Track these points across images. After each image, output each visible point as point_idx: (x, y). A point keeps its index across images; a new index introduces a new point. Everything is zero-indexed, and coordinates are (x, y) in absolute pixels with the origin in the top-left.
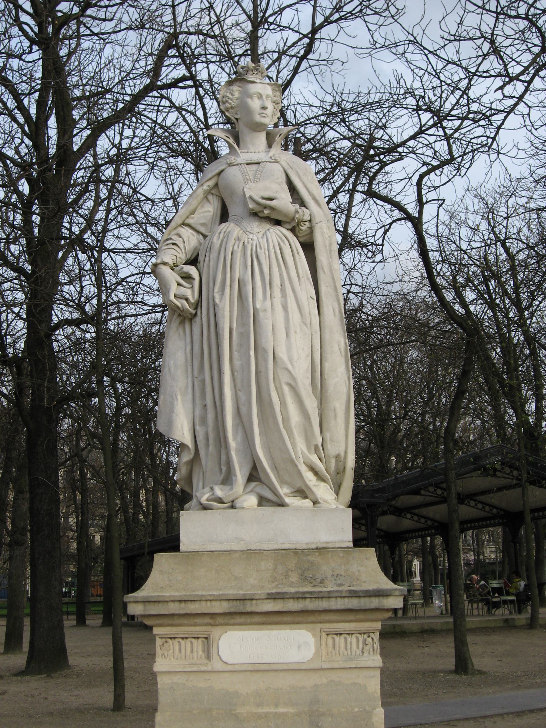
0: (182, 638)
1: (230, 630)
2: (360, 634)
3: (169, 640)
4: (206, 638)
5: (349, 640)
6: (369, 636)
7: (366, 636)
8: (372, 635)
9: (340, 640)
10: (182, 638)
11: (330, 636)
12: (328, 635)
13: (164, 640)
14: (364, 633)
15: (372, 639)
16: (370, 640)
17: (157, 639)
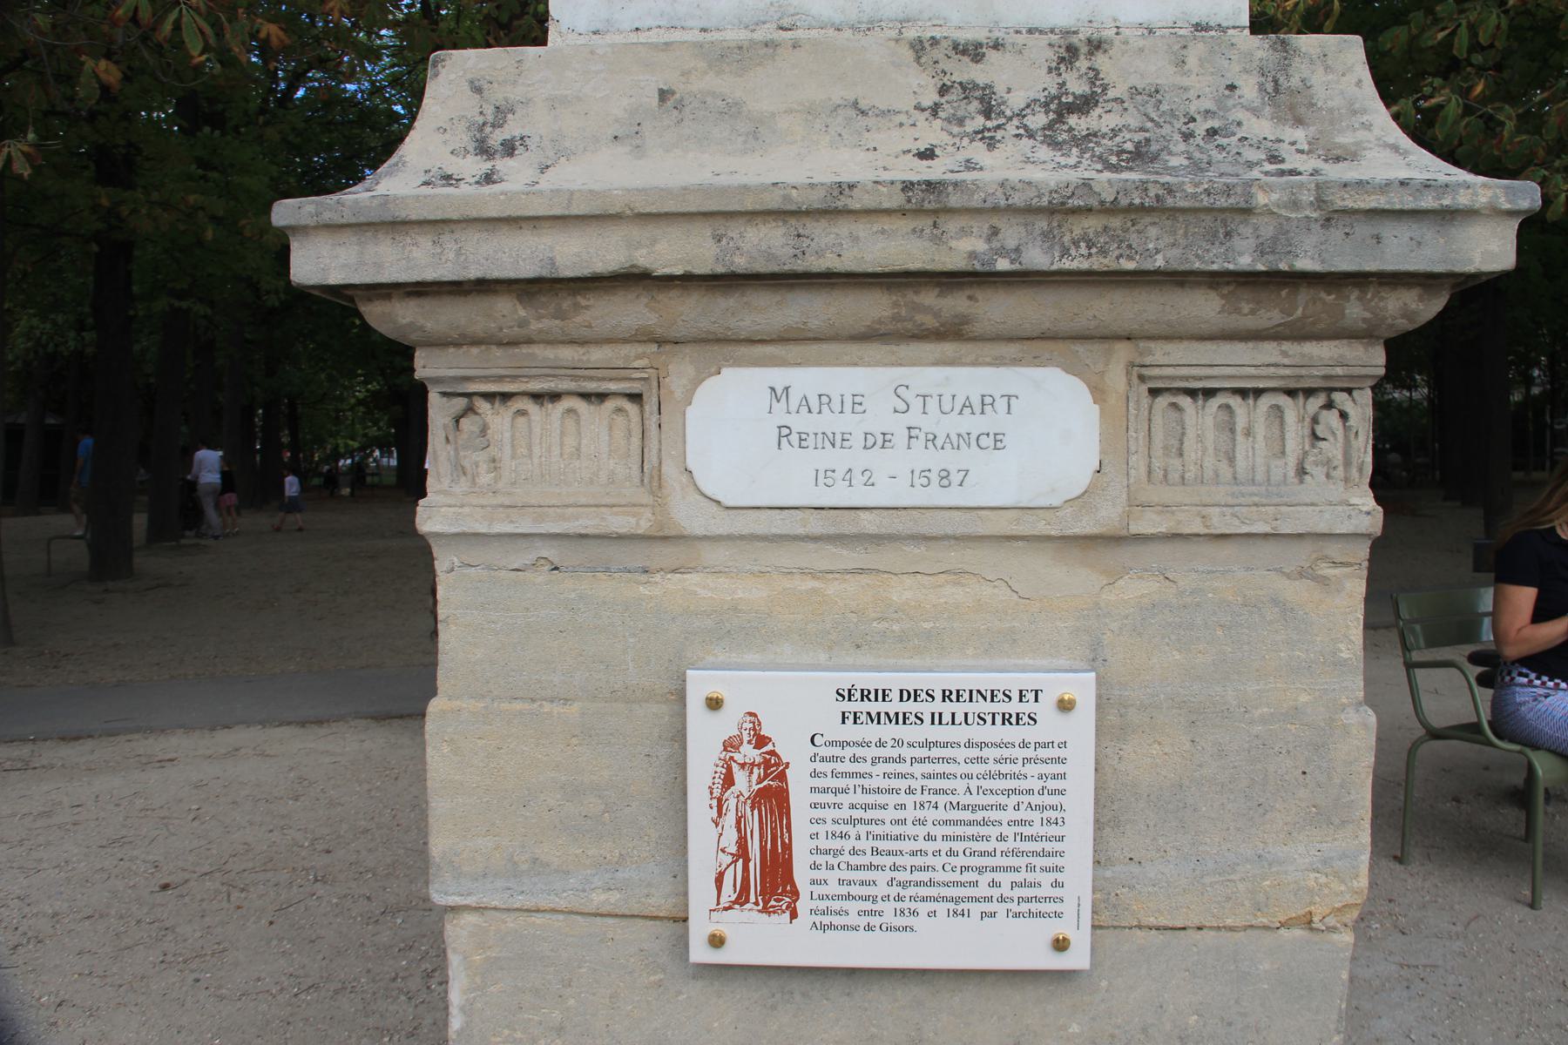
0: (537, 397)
1: (738, 363)
2: (1291, 393)
3: (483, 406)
4: (636, 398)
5: (1241, 422)
6: (1329, 405)
7: (1315, 403)
8: (1339, 397)
9: (1201, 419)
10: (537, 397)
11: (1162, 401)
12: (1154, 392)
13: (461, 403)
14: (1309, 392)
15: (1344, 416)
16: (1331, 418)
17: (434, 398)
